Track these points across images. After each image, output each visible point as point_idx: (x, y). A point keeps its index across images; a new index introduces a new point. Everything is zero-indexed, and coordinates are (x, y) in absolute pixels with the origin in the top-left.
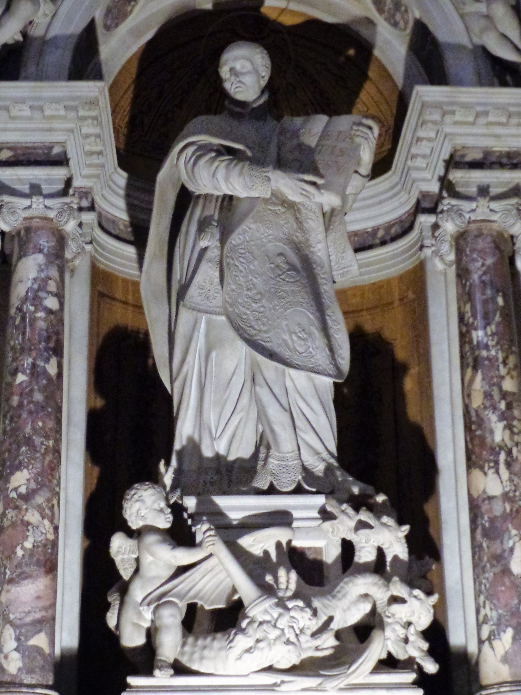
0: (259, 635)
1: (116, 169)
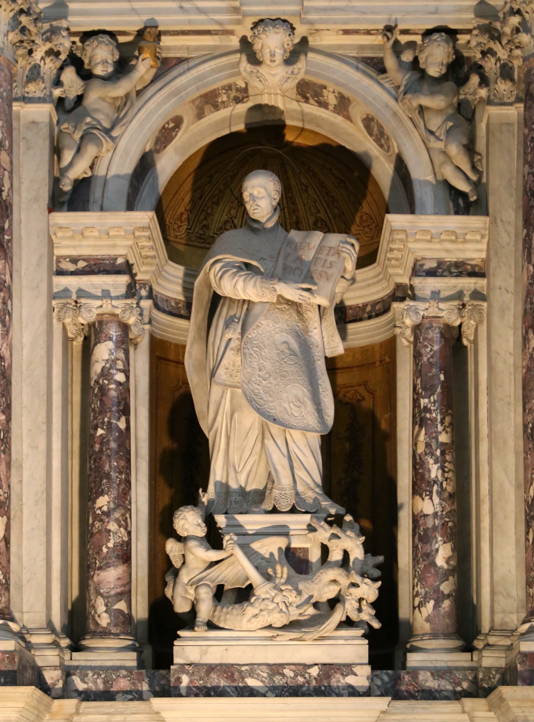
0: (262, 607)
1: (167, 262)
